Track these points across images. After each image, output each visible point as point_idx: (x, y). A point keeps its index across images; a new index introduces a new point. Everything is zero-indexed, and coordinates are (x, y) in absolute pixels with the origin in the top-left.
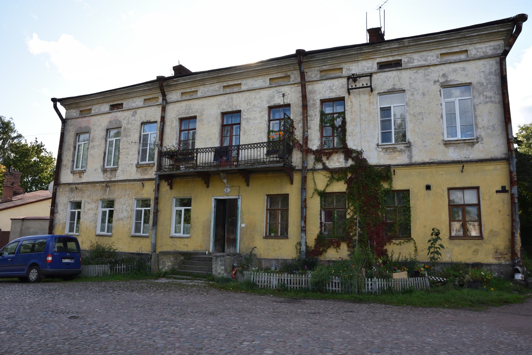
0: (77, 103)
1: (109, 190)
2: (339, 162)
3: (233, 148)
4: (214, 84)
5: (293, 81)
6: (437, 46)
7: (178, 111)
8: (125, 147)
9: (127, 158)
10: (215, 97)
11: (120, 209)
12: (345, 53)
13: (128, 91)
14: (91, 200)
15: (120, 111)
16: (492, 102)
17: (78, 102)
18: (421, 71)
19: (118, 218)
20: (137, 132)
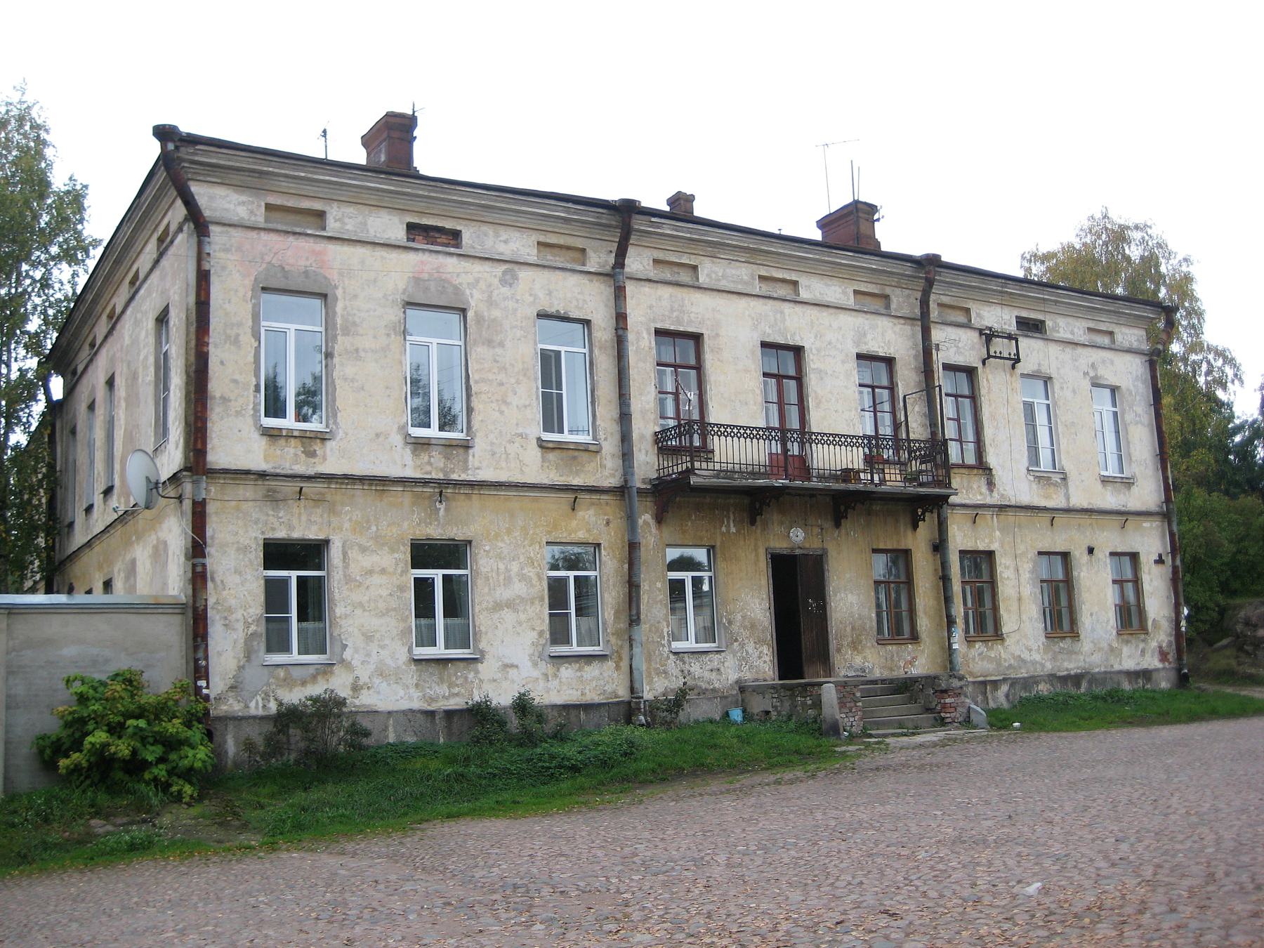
0: (261, 173)
1: (447, 510)
2: (981, 494)
3: (807, 436)
4: (738, 264)
5: (896, 310)
6: (1085, 314)
7: (651, 307)
8: (491, 376)
9: (502, 413)
10: (742, 297)
11: (498, 574)
12: (984, 283)
13: (496, 201)
14: (377, 538)
15: (451, 254)
16: (1141, 422)
17: (268, 173)
18: (1069, 350)
19: (495, 602)
20: (525, 337)
